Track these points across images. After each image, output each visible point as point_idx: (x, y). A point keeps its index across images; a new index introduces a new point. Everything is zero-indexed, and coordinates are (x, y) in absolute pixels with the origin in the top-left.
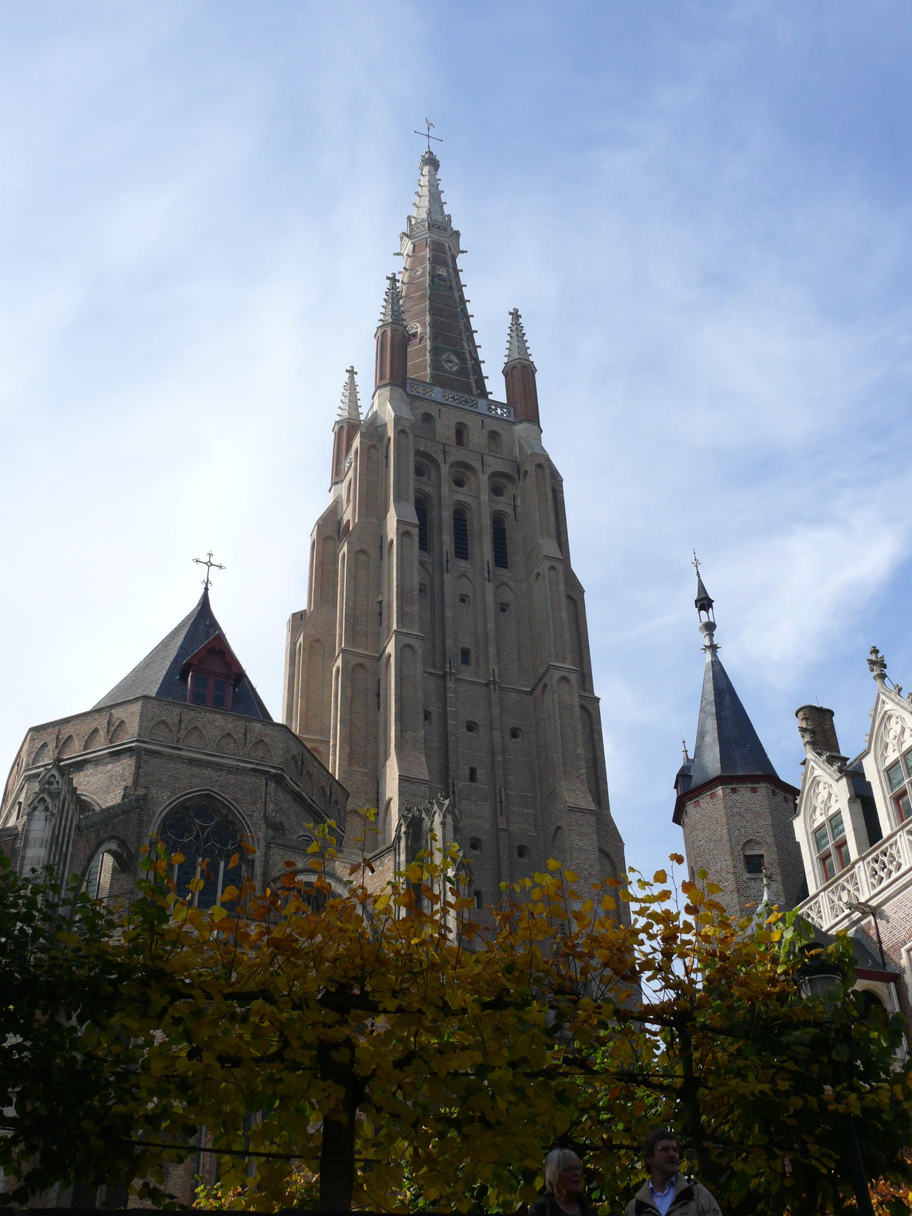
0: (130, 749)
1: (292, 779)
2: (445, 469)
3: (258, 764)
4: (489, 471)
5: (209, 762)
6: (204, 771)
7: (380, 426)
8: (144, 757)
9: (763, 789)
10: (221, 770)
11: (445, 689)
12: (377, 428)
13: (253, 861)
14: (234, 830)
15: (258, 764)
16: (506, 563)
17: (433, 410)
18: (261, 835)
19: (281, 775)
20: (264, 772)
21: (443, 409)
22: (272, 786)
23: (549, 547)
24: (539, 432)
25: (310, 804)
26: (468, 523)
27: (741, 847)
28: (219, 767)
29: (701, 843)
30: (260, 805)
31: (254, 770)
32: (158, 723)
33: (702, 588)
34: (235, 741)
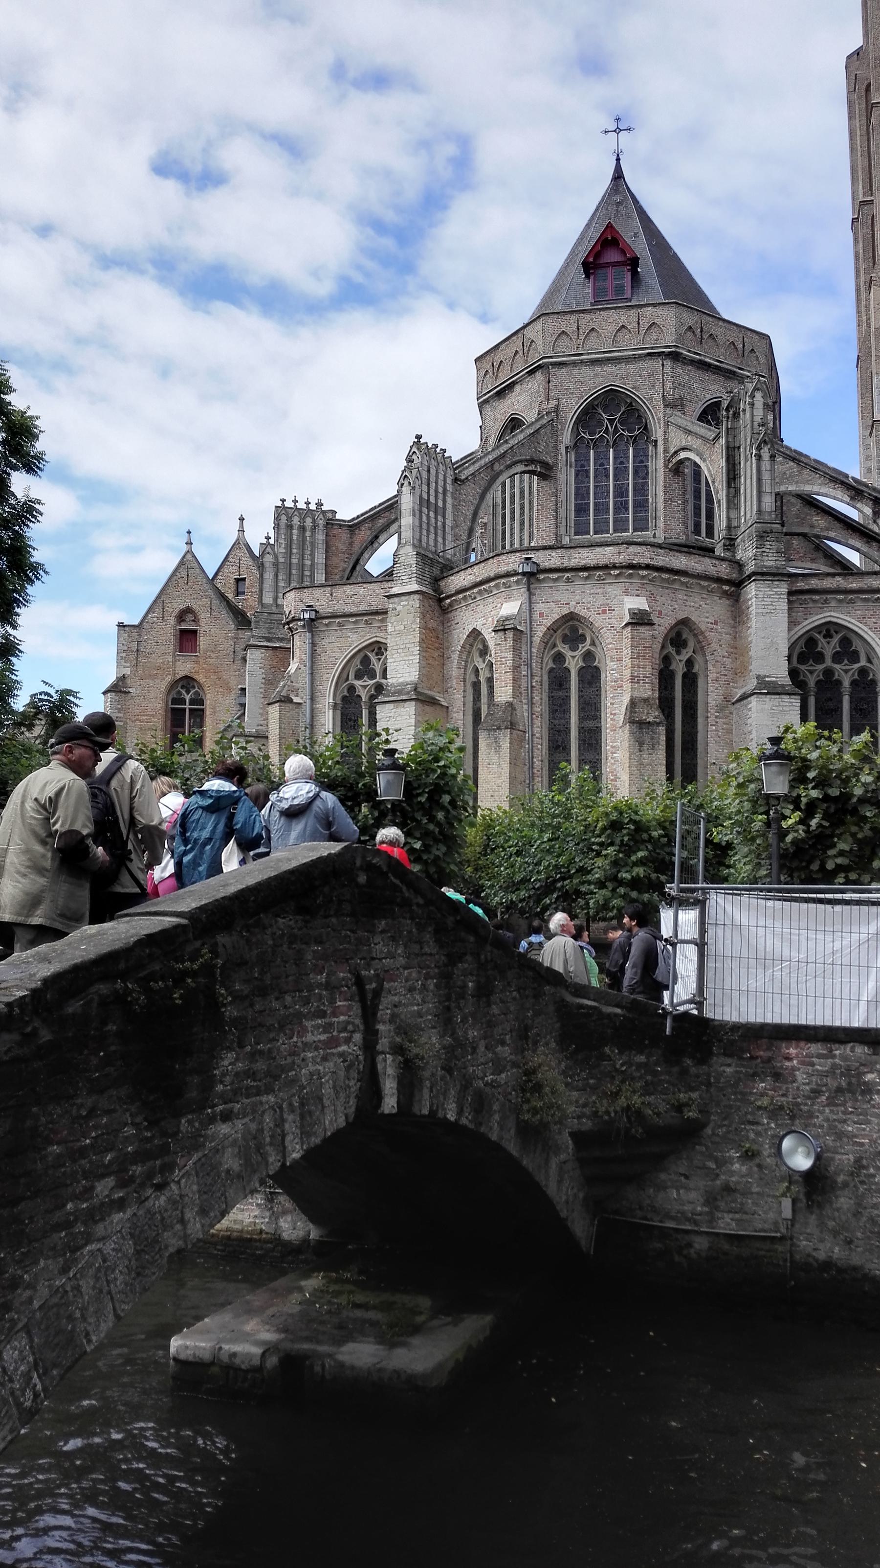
0: (540, 367)
1: (689, 351)
3: (652, 348)
5: (609, 360)
6: (605, 368)
8: (552, 370)
10: (620, 363)
13: (656, 441)
14: (640, 417)
15: (652, 348)
18: (661, 415)
19: (675, 352)
20: (659, 354)
22: (668, 363)
25: (717, 366)
30: (659, 386)
31: (649, 354)
32: (559, 335)
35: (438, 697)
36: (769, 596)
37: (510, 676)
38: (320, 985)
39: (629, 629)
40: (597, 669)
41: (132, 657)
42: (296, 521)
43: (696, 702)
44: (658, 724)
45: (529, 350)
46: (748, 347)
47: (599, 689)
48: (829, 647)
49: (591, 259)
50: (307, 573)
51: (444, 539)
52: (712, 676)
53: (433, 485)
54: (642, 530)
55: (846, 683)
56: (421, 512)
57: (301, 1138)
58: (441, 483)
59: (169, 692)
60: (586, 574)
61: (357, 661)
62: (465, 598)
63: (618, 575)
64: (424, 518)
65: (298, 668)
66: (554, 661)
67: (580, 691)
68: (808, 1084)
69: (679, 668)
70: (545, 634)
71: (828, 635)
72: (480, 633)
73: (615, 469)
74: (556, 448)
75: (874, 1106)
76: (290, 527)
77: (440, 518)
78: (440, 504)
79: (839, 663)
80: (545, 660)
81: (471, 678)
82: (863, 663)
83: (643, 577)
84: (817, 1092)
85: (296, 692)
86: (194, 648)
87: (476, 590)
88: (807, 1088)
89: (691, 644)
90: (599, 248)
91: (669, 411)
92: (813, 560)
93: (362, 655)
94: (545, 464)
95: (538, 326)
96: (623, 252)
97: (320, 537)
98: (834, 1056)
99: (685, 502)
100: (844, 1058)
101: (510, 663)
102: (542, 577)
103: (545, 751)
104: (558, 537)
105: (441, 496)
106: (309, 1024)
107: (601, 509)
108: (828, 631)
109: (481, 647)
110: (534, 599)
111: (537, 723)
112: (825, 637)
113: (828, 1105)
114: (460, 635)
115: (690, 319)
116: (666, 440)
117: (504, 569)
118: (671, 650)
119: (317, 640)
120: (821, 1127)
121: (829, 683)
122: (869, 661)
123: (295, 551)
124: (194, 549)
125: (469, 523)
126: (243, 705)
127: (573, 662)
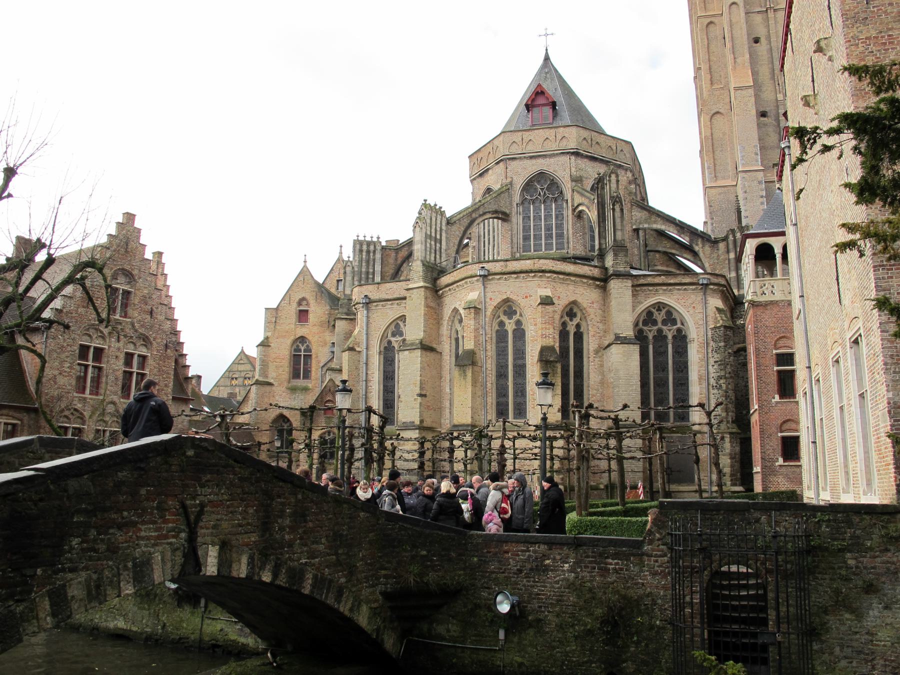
0: (502, 160)
11: (767, 19)
14: (558, 187)
18: (569, 186)
20: (568, 153)
22: (573, 158)
30: (568, 170)
35: (434, 346)
36: (621, 288)
37: (473, 334)
38: (152, 508)
39: (540, 306)
40: (523, 330)
41: (272, 326)
42: (365, 247)
43: (582, 349)
44: (556, 362)
47: (524, 342)
48: (659, 317)
49: (529, 103)
50: (371, 276)
51: (441, 257)
52: (591, 333)
53: (434, 227)
54: (561, 249)
55: (670, 337)
56: (426, 242)
57: (134, 584)
58: (438, 225)
59: (292, 345)
60: (515, 276)
61: (393, 327)
62: (450, 290)
63: (534, 276)
64: (428, 245)
65: (360, 331)
66: (499, 326)
67: (514, 342)
68: (516, 566)
69: (572, 329)
70: (493, 310)
71: (659, 310)
72: (458, 310)
73: (545, 216)
74: (511, 204)
75: (548, 578)
76: (361, 251)
77: (438, 245)
78: (438, 237)
79: (666, 325)
80: (494, 325)
81: (454, 336)
82: (679, 325)
83: (548, 277)
84: (520, 571)
85: (358, 344)
86: (306, 321)
87: (455, 285)
88: (515, 568)
89: (579, 315)
90: (533, 96)
91: (574, 184)
92: (667, 266)
93: (395, 323)
94: (504, 213)
95: (501, 138)
96: (548, 99)
97: (378, 256)
98: (529, 551)
99: (584, 234)
100: (535, 552)
101: (472, 327)
102: (490, 277)
103: (494, 378)
104: (513, 254)
105: (438, 233)
106: (143, 527)
107: (537, 237)
108: (659, 307)
109: (459, 318)
110: (487, 290)
111: (489, 361)
112: (657, 310)
113: (526, 578)
114: (447, 312)
115: (585, 134)
116: (573, 200)
117: (469, 273)
118: (567, 319)
119: (370, 315)
120: (521, 590)
121: (660, 337)
122: (682, 324)
123: (364, 264)
124: (308, 265)
125: (456, 247)
126: (333, 352)
127: (510, 326)
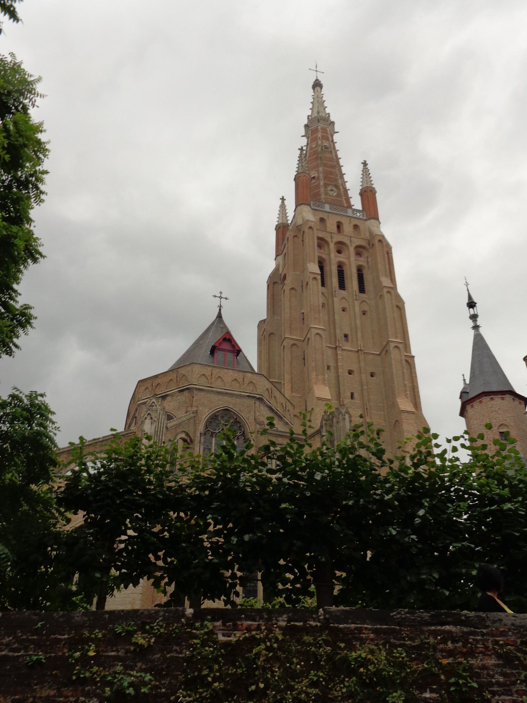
0: (188, 389)
2: (332, 246)
3: (250, 393)
4: (354, 245)
5: (227, 393)
6: (224, 398)
7: (299, 225)
8: (195, 392)
9: (508, 397)
10: (232, 397)
12: (297, 226)
15: (250, 393)
16: (364, 291)
17: (325, 216)
18: (253, 427)
20: (253, 397)
21: (330, 215)
22: (258, 403)
23: (385, 282)
24: (379, 224)
25: (276, 412)
26: (345, 272)
27: (497, 428)
28: (232, 395)
29: (475, 426)
30: (252, 413)
31: (248, 396)
32: (201, 375)
33: (470, 297)
34: (239, 383)
45: (180, 380)
46: (287, 409)
74: (195, 431)
